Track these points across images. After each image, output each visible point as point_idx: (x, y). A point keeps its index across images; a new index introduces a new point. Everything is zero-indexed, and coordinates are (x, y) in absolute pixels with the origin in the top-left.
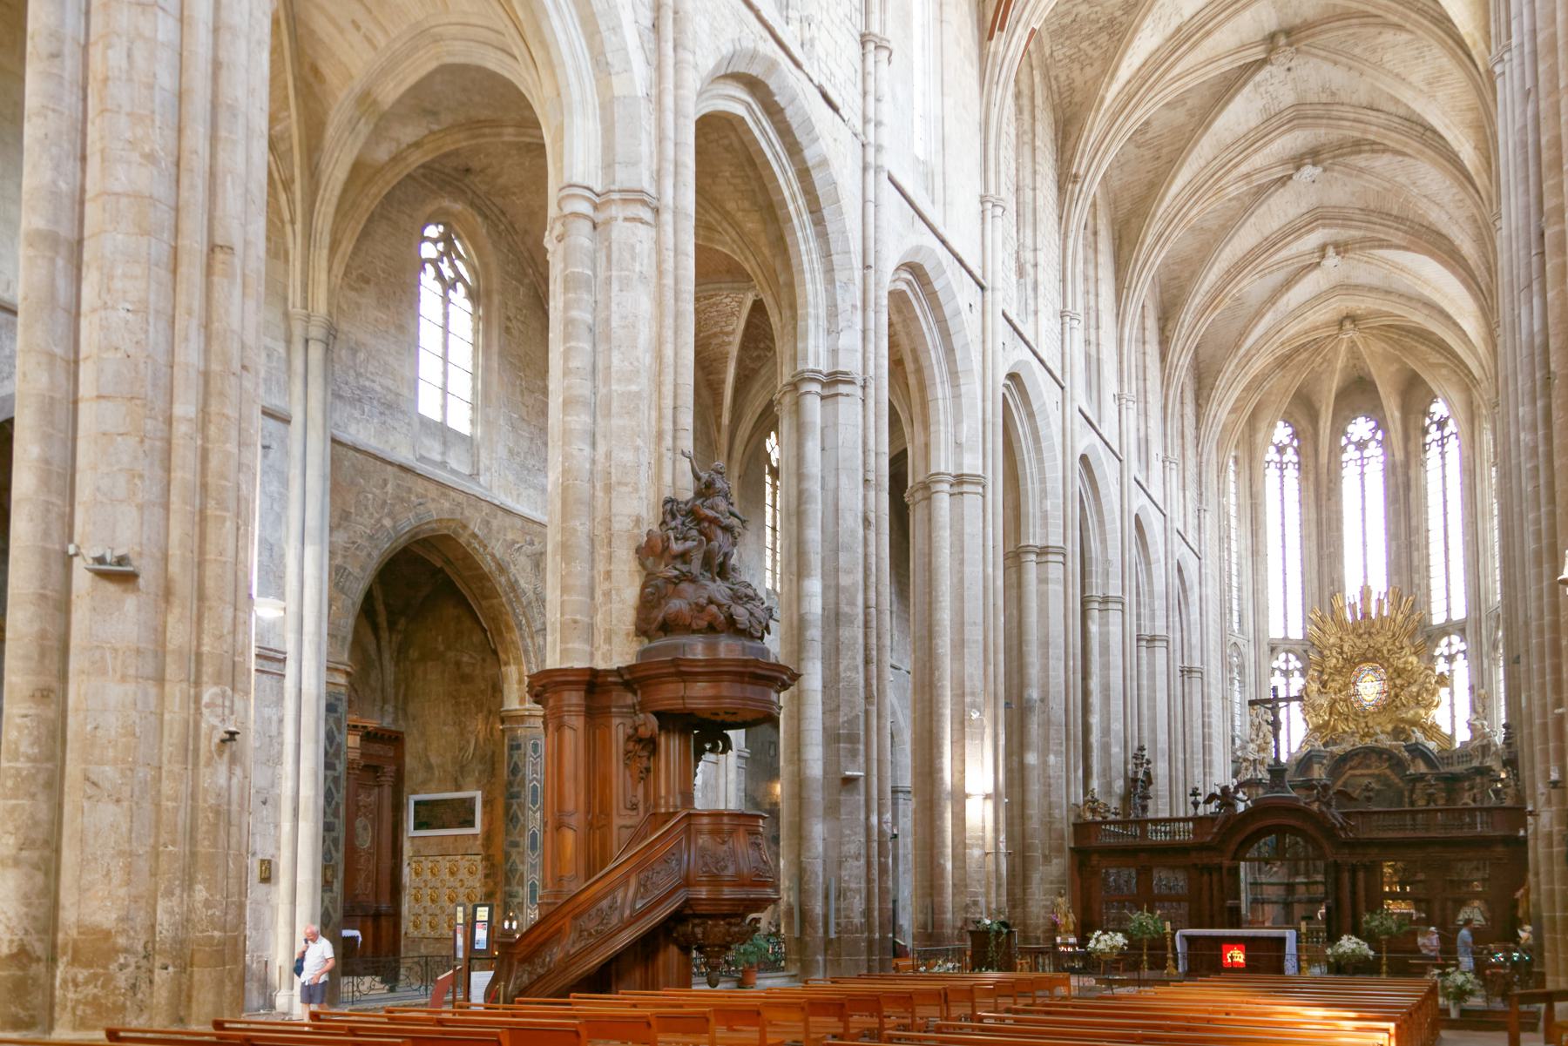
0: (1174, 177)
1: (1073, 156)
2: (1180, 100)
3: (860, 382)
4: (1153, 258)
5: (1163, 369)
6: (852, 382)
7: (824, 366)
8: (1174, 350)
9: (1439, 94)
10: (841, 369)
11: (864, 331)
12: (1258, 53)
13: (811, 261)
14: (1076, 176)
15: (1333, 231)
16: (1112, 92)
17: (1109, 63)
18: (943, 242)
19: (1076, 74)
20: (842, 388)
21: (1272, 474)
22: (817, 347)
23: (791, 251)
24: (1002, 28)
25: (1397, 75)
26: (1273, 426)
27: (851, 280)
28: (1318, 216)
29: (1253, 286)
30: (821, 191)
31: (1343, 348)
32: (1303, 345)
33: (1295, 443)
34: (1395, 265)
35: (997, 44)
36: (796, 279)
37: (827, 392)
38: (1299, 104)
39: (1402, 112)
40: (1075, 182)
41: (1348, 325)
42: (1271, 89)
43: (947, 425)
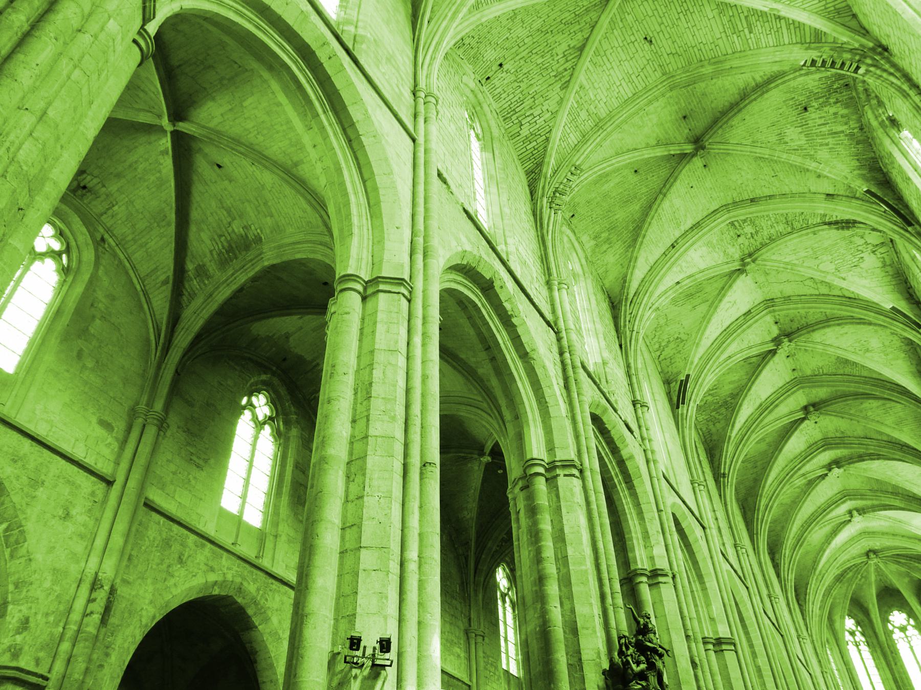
0: (768, 475)
1: (720, 464)
2: (763, 439)
3: (671, 575)
5: (780, 582)
6: (666, 575)
7: (647, 566)
8: (784, 571)
9: (904, 429)
10: (658, 567)
11: (666, 546)
13: (629, 509)
14: (724, 474)
15: (853, 502)
16: (734, 433)
17: (729, 421)
18: (684, 502)
19: (711, 427)
20: (661, 579)
22: (641, 555)
23: (617, 503)
24: (683, 403)
25: (878, 421)
26: (843, 618)
27: (653, 518)
28: (846, 495)
29: (816, 535)
30: (631, 470)
31: (872, 569)
32: (849, 568)
33: (859, 628)
34: (895, 520)
35: (682, 409)
36: (622, 518)
37: (651, 582)
38: (824, 439)
39: (885, 438)
40: (724, 477)
41: (872, 555)
42: (808, 432)
43: (702, 607)
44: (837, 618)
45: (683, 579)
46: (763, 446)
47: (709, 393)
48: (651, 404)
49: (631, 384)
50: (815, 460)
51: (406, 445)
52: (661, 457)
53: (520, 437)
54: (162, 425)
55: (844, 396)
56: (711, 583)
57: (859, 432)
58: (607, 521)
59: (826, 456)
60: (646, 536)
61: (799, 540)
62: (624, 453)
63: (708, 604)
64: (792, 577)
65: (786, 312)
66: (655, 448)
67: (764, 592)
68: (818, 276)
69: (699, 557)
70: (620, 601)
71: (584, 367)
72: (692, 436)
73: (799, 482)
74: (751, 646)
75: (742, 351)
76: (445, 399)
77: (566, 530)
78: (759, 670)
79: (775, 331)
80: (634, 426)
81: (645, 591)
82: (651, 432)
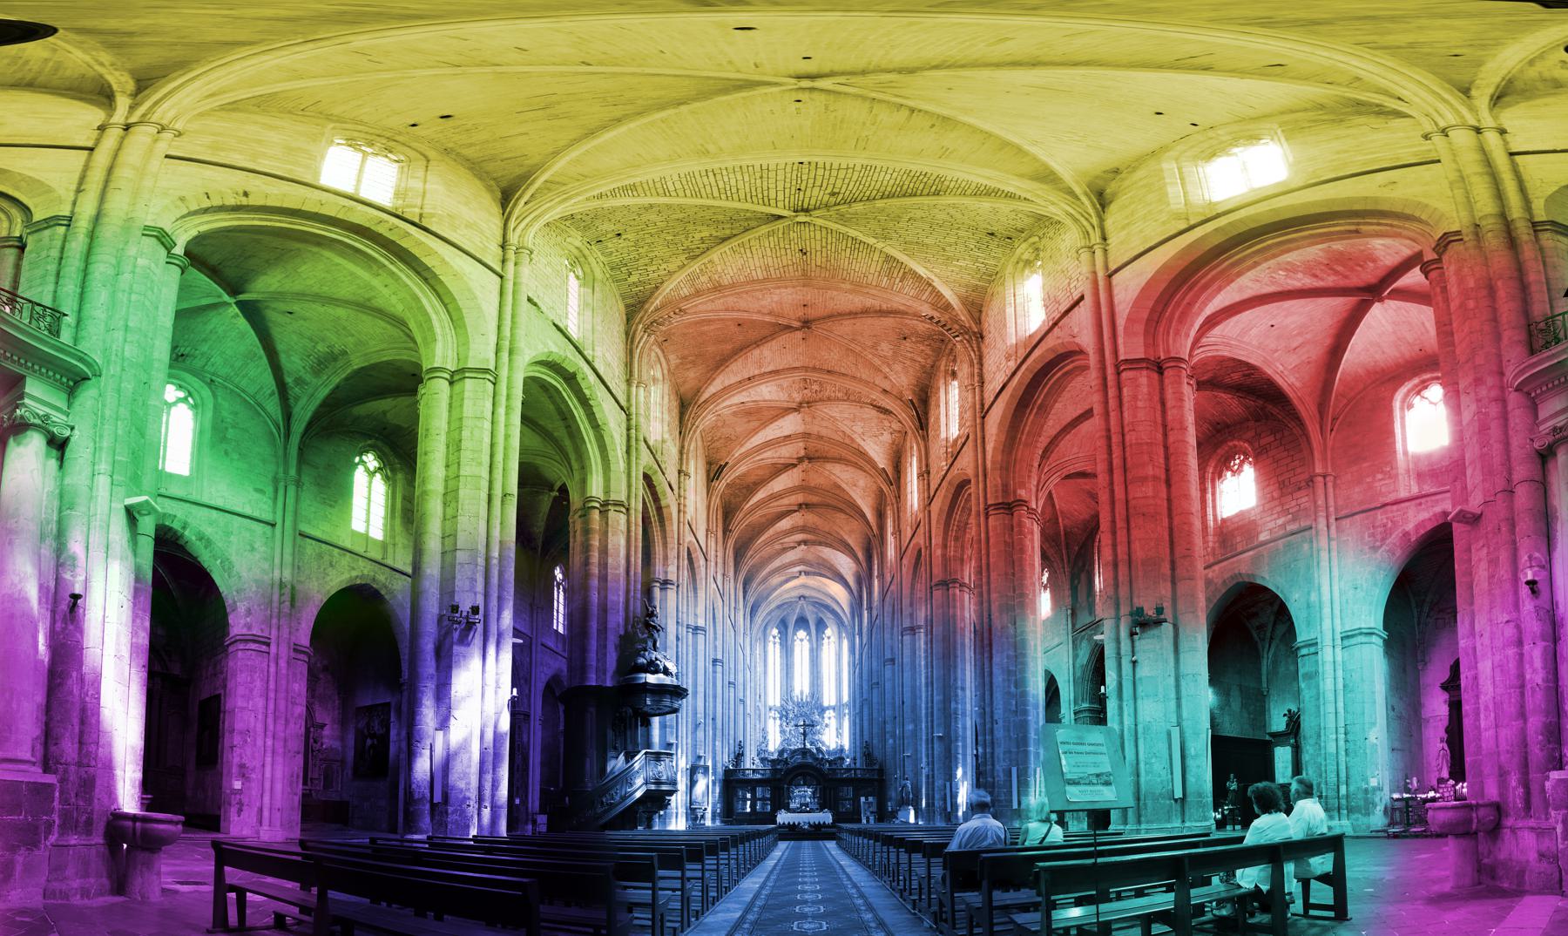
4: (749, 562)
12: (796, 508)
17: (746, 498)
21: (770, 646)
44: (769, 628)
45: (683, 589)
46: (764, 520)
50: (793, 537)
51: (491, 482)
52: (690, 510)
53: (584, 481)
56: (701, 594)
58: (640, 545)
59: (800, 537)
60: (666, 558)
61: (765, 580)
62: (663, 503)
63: (696, 606)
65: (813, 444)
66: (687, 504)
68: (848, 431)
69: (698, 577)
70: (639, 596)
71: (645, 441)
72: (716, 501)
73: (778, 547)
74: (715, 633)
75: (773, 458)
76: (523, 451)
77: (610, 546)
78: (715, 647)
80: (675, 487)
81: (657, 592)
82: (687, 501)
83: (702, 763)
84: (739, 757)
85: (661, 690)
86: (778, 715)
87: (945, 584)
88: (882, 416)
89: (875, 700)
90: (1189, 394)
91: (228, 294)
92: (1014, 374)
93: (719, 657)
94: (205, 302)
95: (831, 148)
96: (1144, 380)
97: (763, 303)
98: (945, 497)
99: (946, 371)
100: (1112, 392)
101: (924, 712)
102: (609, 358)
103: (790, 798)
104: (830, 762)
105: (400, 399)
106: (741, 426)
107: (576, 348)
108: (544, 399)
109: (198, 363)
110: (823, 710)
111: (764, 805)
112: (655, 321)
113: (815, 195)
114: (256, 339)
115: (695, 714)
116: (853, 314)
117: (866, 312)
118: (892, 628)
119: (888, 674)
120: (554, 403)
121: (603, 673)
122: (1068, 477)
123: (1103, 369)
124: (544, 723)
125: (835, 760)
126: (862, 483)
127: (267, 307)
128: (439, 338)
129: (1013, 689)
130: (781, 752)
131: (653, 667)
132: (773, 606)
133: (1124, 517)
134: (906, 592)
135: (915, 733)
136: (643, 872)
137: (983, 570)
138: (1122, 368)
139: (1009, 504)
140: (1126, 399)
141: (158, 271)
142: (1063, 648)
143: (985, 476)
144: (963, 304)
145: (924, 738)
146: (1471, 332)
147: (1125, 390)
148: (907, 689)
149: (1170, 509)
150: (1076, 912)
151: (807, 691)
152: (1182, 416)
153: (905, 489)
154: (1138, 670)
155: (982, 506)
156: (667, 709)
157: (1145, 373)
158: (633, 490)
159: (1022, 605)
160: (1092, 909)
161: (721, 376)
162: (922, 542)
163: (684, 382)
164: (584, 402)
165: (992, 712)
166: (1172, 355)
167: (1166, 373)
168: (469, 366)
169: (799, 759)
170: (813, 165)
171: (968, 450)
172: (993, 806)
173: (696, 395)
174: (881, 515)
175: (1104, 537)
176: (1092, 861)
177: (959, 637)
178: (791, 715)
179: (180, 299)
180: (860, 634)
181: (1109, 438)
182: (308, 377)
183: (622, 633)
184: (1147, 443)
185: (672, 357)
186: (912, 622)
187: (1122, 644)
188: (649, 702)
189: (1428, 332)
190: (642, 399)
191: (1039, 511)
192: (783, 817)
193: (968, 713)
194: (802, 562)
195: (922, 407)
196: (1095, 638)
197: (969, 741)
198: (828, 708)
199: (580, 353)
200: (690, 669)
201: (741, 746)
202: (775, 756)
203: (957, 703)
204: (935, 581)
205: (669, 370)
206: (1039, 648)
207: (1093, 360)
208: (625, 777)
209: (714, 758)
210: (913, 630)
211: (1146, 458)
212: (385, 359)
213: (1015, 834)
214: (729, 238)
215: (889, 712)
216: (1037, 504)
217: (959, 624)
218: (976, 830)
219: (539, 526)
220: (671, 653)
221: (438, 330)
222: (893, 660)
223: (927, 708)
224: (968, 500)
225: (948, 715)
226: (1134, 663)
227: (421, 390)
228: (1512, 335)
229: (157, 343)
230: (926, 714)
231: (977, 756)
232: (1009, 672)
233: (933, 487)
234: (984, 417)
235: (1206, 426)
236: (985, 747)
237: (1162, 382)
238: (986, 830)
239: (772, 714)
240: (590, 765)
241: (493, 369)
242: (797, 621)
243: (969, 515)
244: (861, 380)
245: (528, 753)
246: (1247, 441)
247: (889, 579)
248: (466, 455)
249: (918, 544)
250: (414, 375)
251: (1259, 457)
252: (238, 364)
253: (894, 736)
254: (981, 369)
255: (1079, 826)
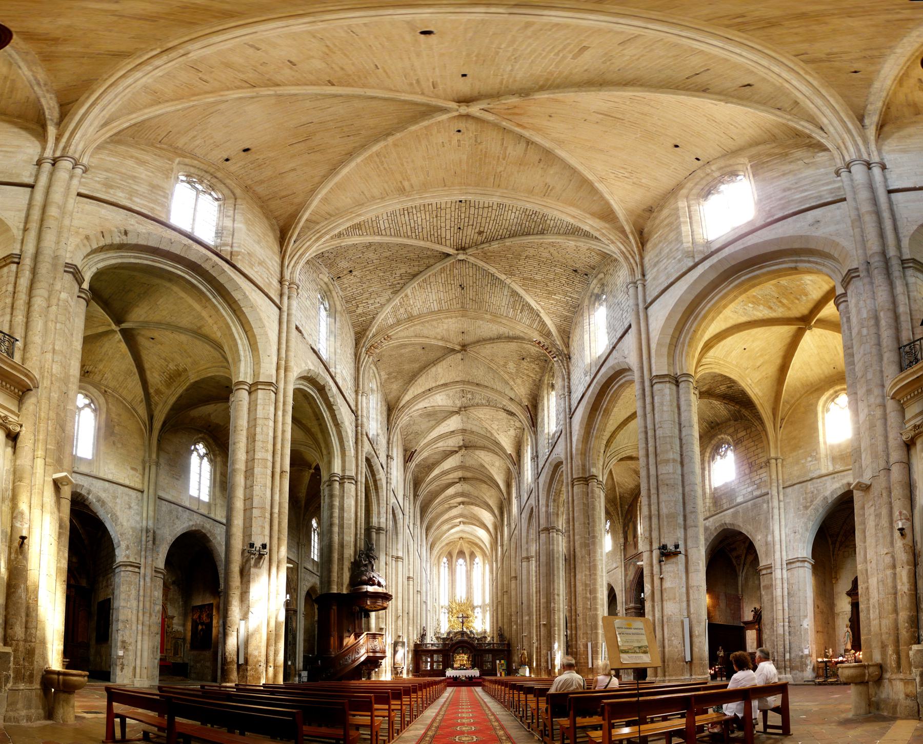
4: (429, 516)
12: (457, 480)
17: (428, 474)
45: (390, 533)
46: (438, 488)
47: (423, 460)
48: (395, 459)
49: (388, 447)
51: (274, 463)
52: (394, 482)
53: (330, 463)
54: (157, 464)
55: (477, 479)
57: (476, 495)
58: (364, 504)
59: (460, 499)
60: (379, 513)
61: (439, 527)
62: (378, 477)
64: (431, 540)
66: (392, 477)
67: (419, 543)
69: (398, 526)
70: (363, 537)
72: (409, 476)
73: (446, 506)
74: (409, 561)
77: (345, 506)
78: (409, 569)
79: (461, 443)
80: (385, 466)
81: (374, 535)
83: (401, 640)
84: (423, 636)
85: (376, 596)
86: (446, 611)
87: (547, 530)
88: (510, 417)
89: (505, 602)
90: (694, 399)
91: (115, 323)
92: (589, 386)
93: (411, 575)
94: (101, 330)
95: (478, 185)
96: (665, 391)
97: (438, 330)
98: (548, 473)
99: (548, 384)
100: (648, 400)
101: (534, 609)
102: (345, 374)
103: (454, 661)
104: (478, 639)
105: (219, 405)
106: (424, 424)
107: (325, 366)
108: (306, 405)
109: (97, 378)
110: (473, 608)
111: (438, 665)
112: (372, 345)
113: (470, 234)
114: (132, 359)
115: (397, 610)
116: (492, 340)
117: (499, 338)
118: (516, 558)
119: (513, 586)
120: (312, 408)
121: (341, 584)
122: (621, 460)
123: (643, 382)
124: (306, 616)
125: (481, 638)
126: (497, 464)
127: (139, 334)
128: (242, 358)
129: (588, 595)
130: (449, 634)
131: (371, 582)
132: (444, 543)
133: (655, 486)
134: (524, 534)
135: (529, 622)
136: (366, 706)
137: (570, 521)
138: (654, 382)
139: (586, 478)
140: (656, 405)
141: (72, 304)
142: (619, 570)
143: (572, 459)
144: (559, 331)
145: (535, 625)
146: (865, 354)
147: (656, 398)
148: (525, 595)
149: (683, 482)
150: (626, 730)
151: (464, 596)
152: (690, 417)
153: (524, 468)
154: (664, 583)
155: (570, 479)
156: (380, 607)
157: (668, 385)
158: (360, 469)
159: (594, 543)
160: (636, 728)
161: (412, 388)
162: (533, 503)
163: (390, 392)
164: (330, 406)
165: (576, 609)
166: (685, 372)
167: (680, 385)
168: (261, 380)
169: (459, 637)
170: (468, 203)
171: (562, 441)
172: (577, 666)
173: (397, 402)
174: (508, 486)
175: (643, 500)
176: (636, 699)
177: (555, 563)
178: (455, 611)
179: (86, 327)
180: (497, 561)
181: (646, 433)
182: (163, 388)
183: (353, 560)
184: (669, 436)
185: (382, 373)
186: (527, 553)
187: (654, 568)
188: (369, 603)
189: (838, 354)
190: (364, 405)
191: (604, 482)
192: (450, 673)
193: (561, 609)
194: (461, 516)
195: (533, 410)
196: (638, 563)
197: (562, 627)
198: (477, 607)
199: (328, 370)
200: (394, 583)
201: (424, 630)
202: (445, 636)
203: (554, 603)
204: (541, 528)
205: (381, 383)
206: (604, 570)
207: (636, 376)
208: (354, 648)
209: (408, 637)
210: (528, 559)
211: (669, 446)
212: (209, 375)
213: (590, 683)
214: (417, 274)
215: (513, 609)
216: (603, 478)
217: (556, 556)
218: (566, 681)
219: (303, 493)
220: (382, 573)
221: (242, 353)
222: (516, 577)
223: (536, 607)
224: (561, 475)
225: (549, 611)
226: (662, 579)
227: (232, 399)
228: (889, 356)
229: (73, 362)
230: (536, 610)
231: (566, 636)
232: (586, 585)
233: (540, 466)
234: (571, 418)
235: (705, 424)
236: (571, 631)
237: (678, 392)
238: (572, 681)
239: (443, 610)
240: (333, 641)
241: (274, 381)
242: (458, 553)
243: (562, 485)
244: (497, 391)
245: (296, 634)
246: (729, 435)
247: (513, 526)
248: (259, 445)
249: (531, 504)
250: (227, 387)
251: (737, 443)
252: (121, 379)
253: (516, 624)
254: (569, 383)
255: (628, 678)
